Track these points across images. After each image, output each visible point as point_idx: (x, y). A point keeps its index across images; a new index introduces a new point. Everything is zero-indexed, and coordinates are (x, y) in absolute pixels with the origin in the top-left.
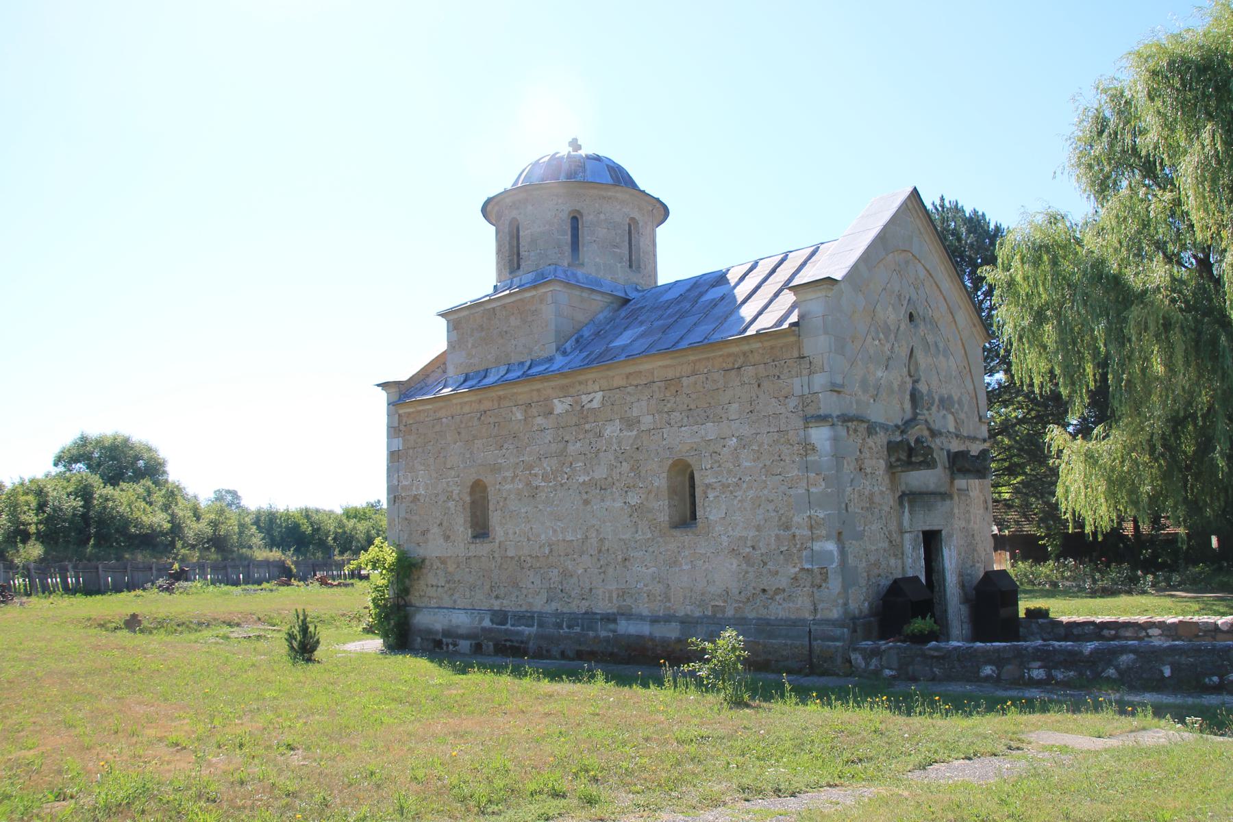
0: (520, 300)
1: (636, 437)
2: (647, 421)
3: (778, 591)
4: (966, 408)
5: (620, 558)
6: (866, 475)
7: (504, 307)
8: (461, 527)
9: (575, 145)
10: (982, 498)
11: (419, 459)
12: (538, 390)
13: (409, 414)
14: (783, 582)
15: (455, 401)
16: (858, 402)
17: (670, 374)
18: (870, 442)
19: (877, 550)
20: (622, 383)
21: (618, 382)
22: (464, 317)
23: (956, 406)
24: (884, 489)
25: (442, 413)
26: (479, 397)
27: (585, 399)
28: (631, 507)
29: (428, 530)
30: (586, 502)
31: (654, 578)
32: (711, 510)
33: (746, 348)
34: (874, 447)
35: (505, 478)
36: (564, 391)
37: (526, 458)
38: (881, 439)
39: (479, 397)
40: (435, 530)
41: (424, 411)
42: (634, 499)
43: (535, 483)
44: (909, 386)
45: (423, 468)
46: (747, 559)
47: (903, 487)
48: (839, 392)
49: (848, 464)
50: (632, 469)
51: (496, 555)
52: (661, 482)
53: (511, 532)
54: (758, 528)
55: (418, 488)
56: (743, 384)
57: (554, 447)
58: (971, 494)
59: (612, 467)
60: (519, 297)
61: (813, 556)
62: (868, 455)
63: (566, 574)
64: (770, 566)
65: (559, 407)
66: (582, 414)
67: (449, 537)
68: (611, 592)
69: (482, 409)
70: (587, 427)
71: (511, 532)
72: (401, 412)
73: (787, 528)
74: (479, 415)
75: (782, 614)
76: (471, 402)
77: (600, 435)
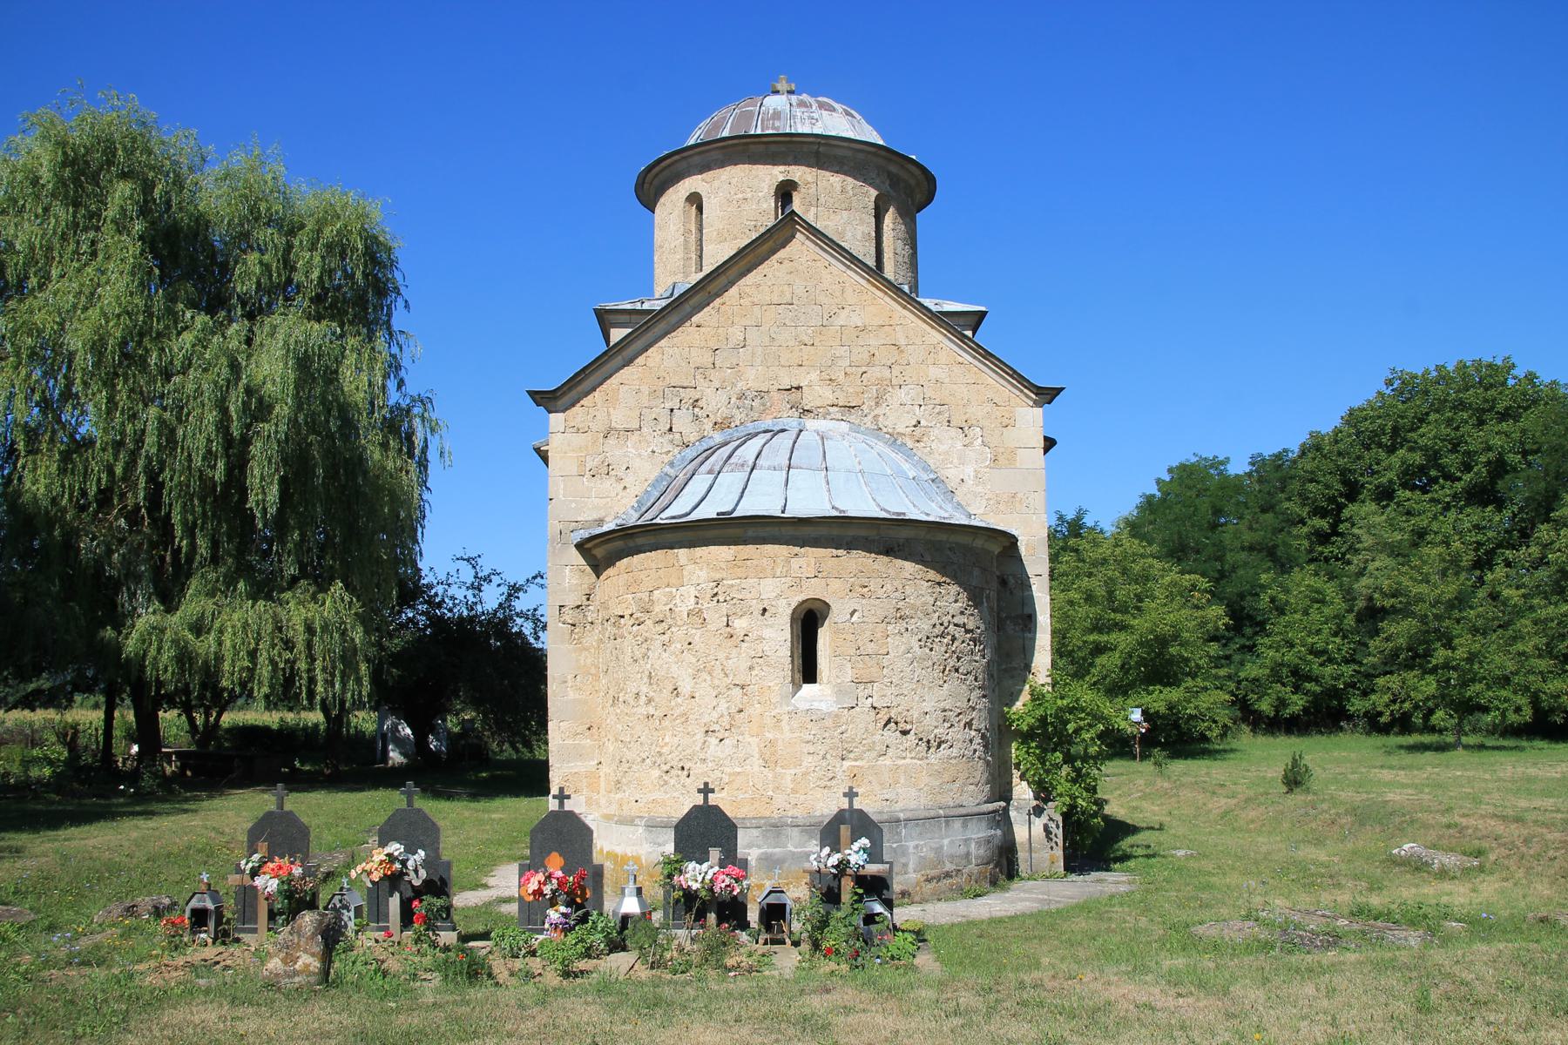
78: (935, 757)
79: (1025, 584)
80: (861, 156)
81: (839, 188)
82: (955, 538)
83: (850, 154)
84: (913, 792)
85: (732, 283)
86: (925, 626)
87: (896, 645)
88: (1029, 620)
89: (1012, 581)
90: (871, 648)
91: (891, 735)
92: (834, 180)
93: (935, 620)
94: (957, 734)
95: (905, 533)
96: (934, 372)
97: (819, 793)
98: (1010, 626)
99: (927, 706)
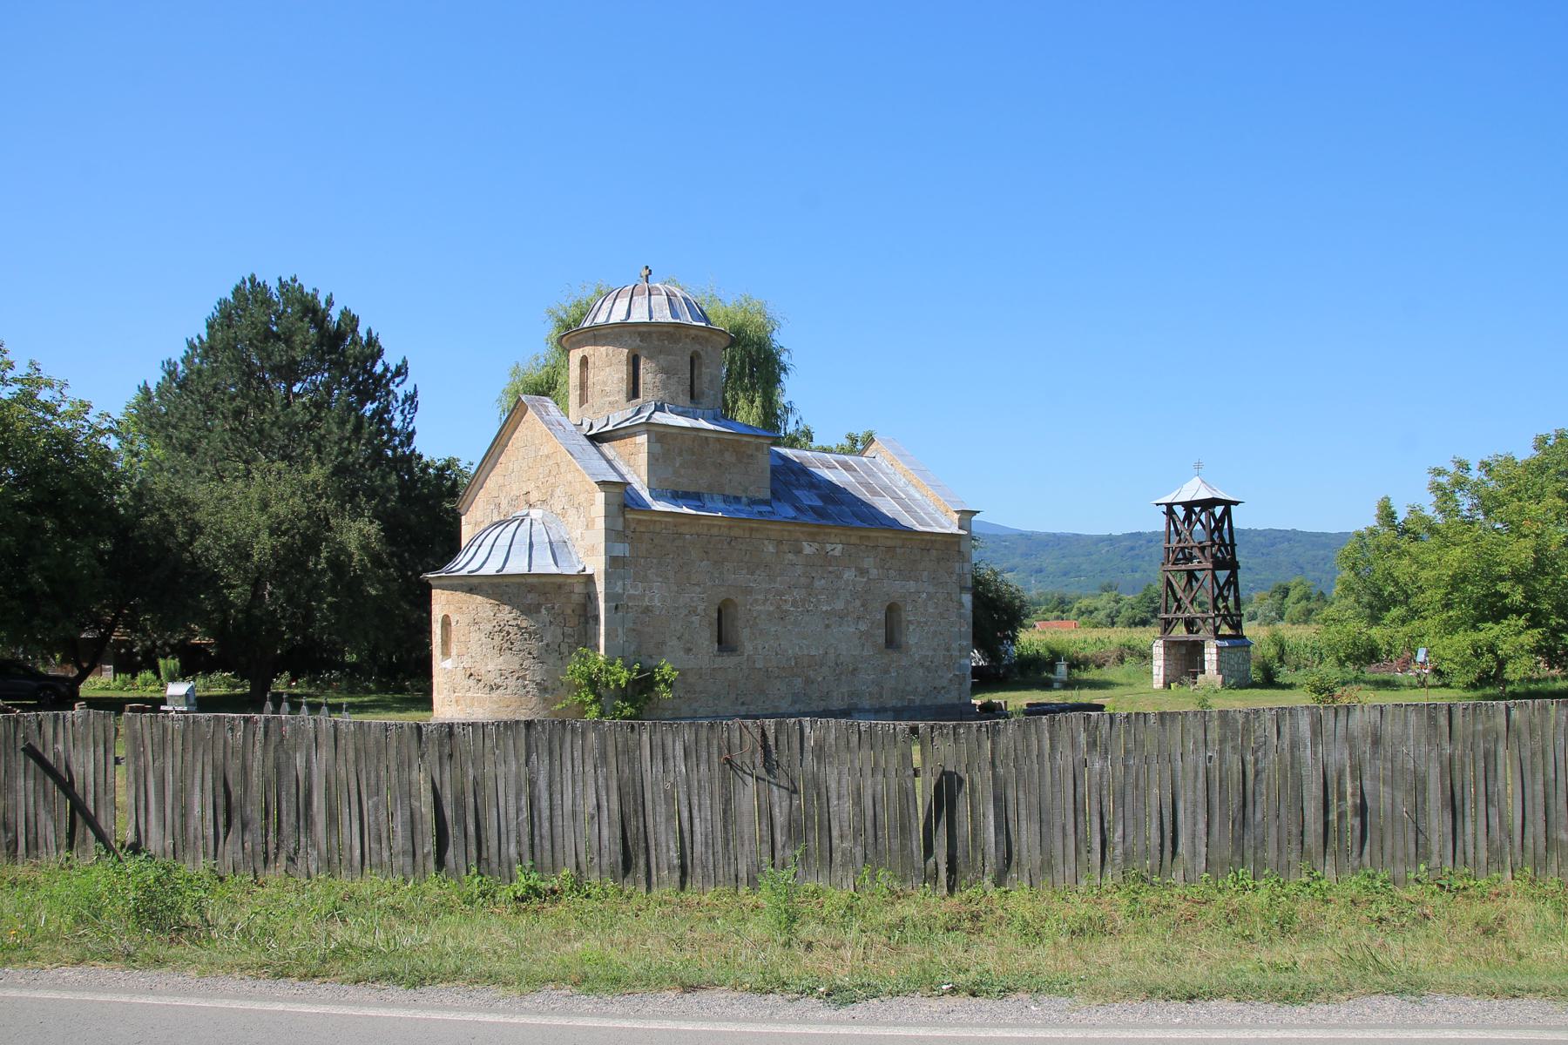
0: (737, 441)
1: (866, 583)
2: (874, 572)
3: (944, 688)
5: (851, 668)
7: (718, 440)
8: (706, 640)
11: (652, 570)
12: (789, 531)
13: (640, 521)
14: (945, 683)
15: (702, 521)
17: (889, 543)
20: (858, 542)
21: (854, 540)
22: (671, 433)
25: (682, 530)
26: (732, 524)
27: (829, 547)
28: (861, 632)
29: (664, 643)
30: (827, 626)
31: (873, 683)
32: (911, 637)
33: (933, 538)
35: (756, 601)
36: (812, 538)
37: (777, 585)
39: (732, 524)
40: (675, 642)
41: (661, 522)
42: (863, 627)
43: (784, 608)
45: (660, 580)
46: (928, 669)
50: (862, 606)
51: (744, 667)
52: (881, 616)
53: (760, 647)
54: (935, 650)
55: (651, 599)
56: (930, 560)
57: (803, 580)
59: (847, 602)
60: (736, 438)
61: (961, 667)
63: (808, 681)
64: (939, 673)
65: (808, 549)
66: (827, 559)
67: (690, 650)
68: (843, 693)
69: (732, 534)
70: (831, 569)
71: (760, 647)
72: (627, 516)
73: (948, 651)
74: (729, 539)
75: (944, 701)
76: (720, 526)
77: (839, 577)
78: (495, 694)
79: (597, 599)
80: (616, 330)
81: (604, 353)
82: (506, 580)
83: (609, 331)
84: (481, 711)
85: (510, 438)
86: (489, 627)
87: (475, 636)
88: (597, 618)
89: (592, 596)
90: (463, 639)
91: (472, 682)
92: (603, 349)
93: (495, 623)
94: (512, 682)
95: (476, 581)
96: (569, 477)
97: (447, 708)
98: (591, 621)
99: (489, 668)
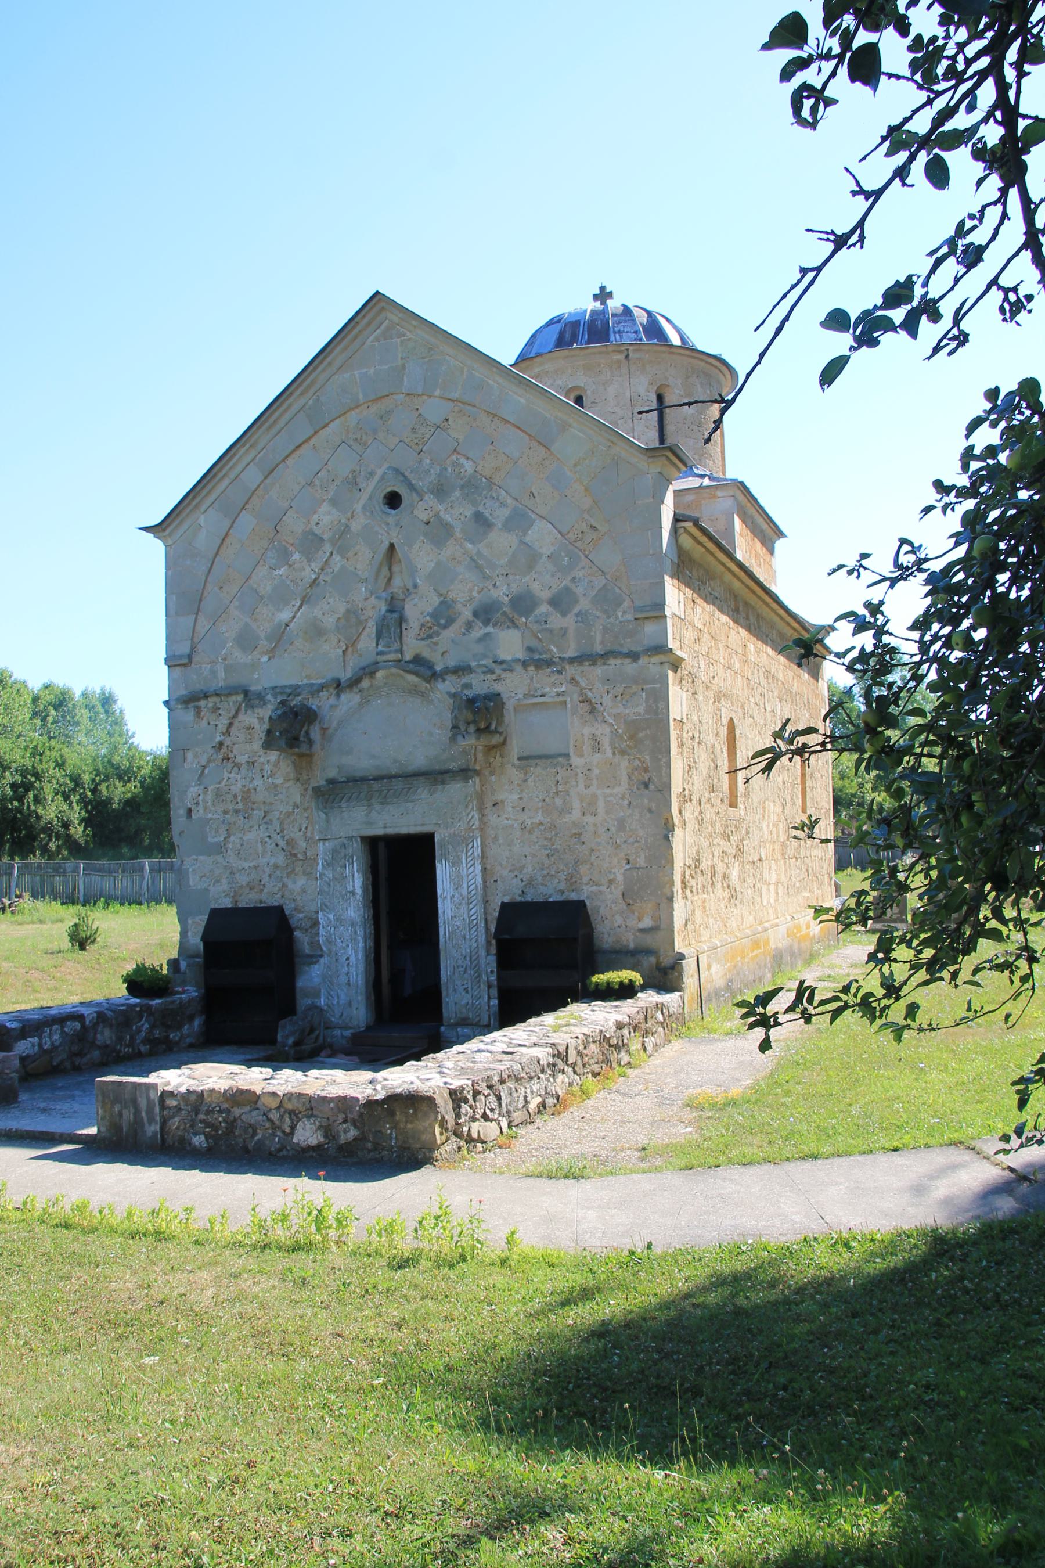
4: (584, 604)
6: (238, 766)
9: (603, 295)
10: (624, 765)
16: (228, 669)
18: (249, 718)
19: (255, 867)
23: (544, 608)
24: (279, 781)
34: (257, 726)
38: (266, 712)
44: (375, 608)
47: (332, 774)
48: (184, 665)
49: (196, 756)
58: (576, 761)
62: (242, 737)
